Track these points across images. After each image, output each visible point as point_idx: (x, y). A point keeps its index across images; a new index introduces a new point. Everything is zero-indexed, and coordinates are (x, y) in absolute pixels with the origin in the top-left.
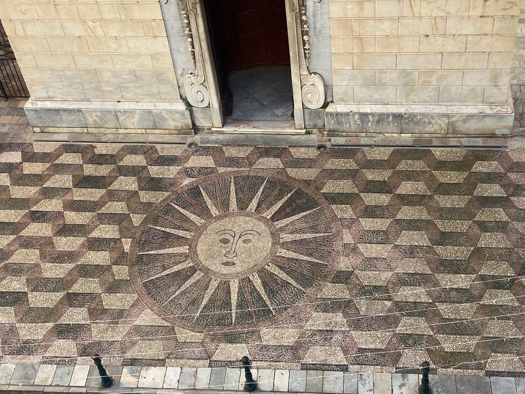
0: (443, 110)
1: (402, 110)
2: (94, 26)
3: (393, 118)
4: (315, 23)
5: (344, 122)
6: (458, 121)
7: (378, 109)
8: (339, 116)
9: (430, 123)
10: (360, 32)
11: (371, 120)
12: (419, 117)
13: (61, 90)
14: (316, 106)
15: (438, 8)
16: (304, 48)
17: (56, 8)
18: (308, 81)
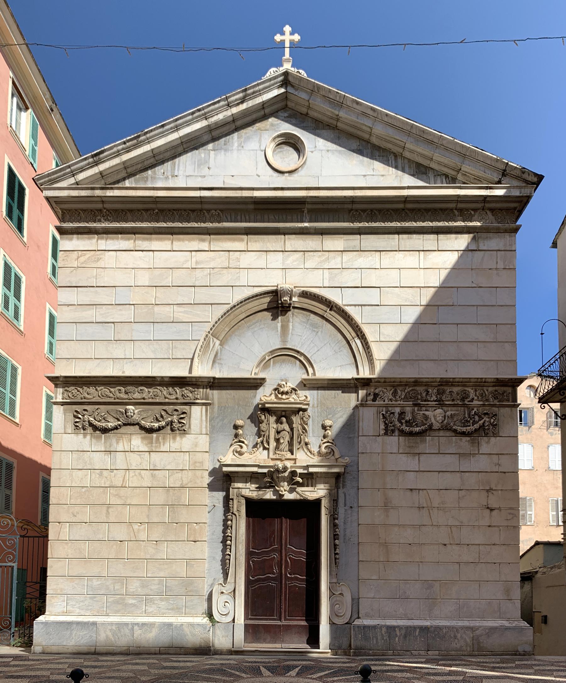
0: (466, 623)
1: (427, 623)
2: (139, 529)
3: (419, 632)
4: (345, 530)
5: (371, 637)
6: (481, 635)
7: (404, 622)
8: (366, 630)
9: (455, 637)
10: (385, 540)
11: (398, 635)
12: (444, 631)
13: (82, 604)
14: (342, 620)
15: (453, 517)
16: (335, 553)
17: (108, 511)
18: (336, 591)
